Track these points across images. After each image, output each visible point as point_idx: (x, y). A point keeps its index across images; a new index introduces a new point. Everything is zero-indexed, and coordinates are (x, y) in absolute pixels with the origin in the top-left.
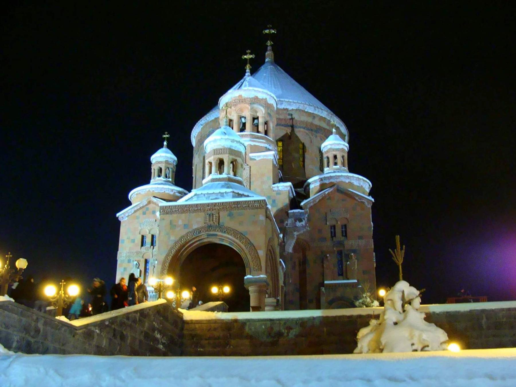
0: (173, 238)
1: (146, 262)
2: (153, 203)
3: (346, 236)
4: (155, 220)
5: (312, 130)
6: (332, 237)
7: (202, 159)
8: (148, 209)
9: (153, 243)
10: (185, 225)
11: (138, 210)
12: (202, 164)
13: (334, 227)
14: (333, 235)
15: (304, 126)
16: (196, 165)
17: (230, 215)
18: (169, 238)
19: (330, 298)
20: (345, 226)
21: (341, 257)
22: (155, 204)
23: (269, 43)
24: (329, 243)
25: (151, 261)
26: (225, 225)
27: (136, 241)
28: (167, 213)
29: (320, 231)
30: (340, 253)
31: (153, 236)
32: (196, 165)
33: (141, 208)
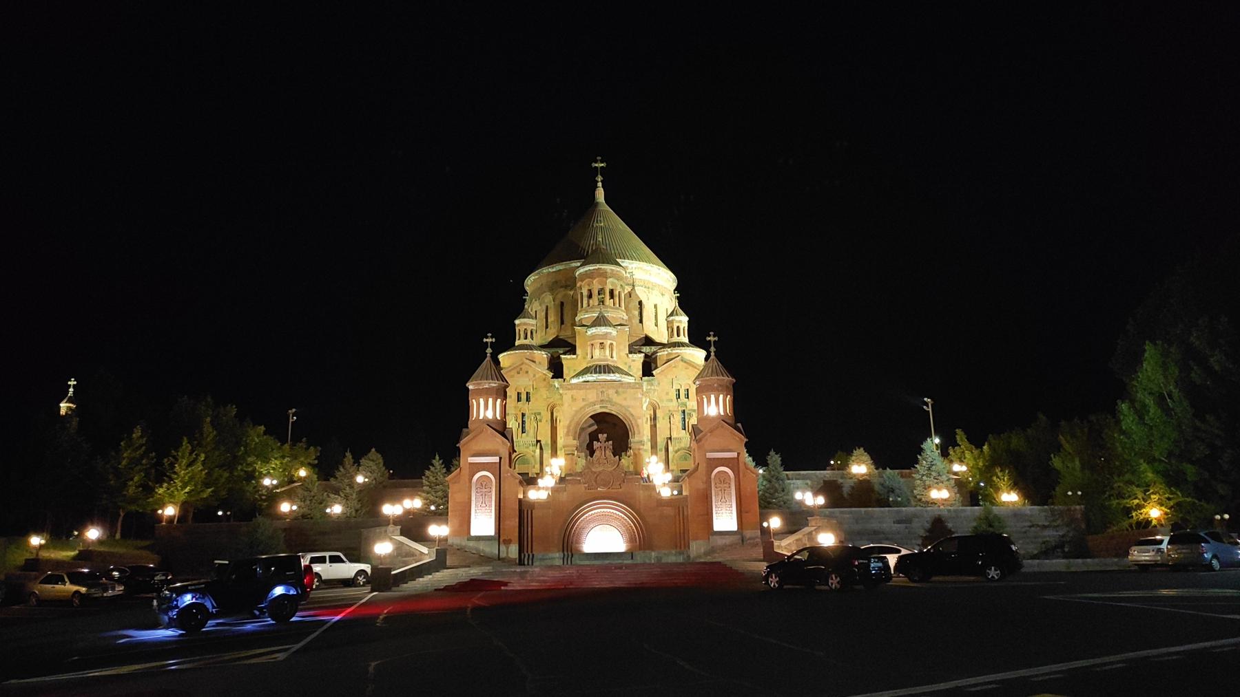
0: (574, 409)
1: (523, 415)
2: (526, 364)
3: (688, 398)
4: (527, 379)
5: (649, 288)
6: (677, 399)
7: (544, 308)
8: (521, 369)
9: (528, 399)
10: (583, 399)
11: (510, 371)
12: (544, 314)
13: (679, 390)
14: (678, 397)
15: (642, 284)
16: (536, 311)
17: (617, 392)
18: (571, 408)
19: (676, 448)
20: (688, 390)
21: (684, 415)
22: (529, 365)
23: (599, 178)
24: (675, 403)
25: (527, 413)
26: (614, 400)
27: (513, 397)
28: (569, 389)
29: (667, 394)
30: (684, 412)
31: (527, 393)
32: (536, 311)
33: (515, 368)
